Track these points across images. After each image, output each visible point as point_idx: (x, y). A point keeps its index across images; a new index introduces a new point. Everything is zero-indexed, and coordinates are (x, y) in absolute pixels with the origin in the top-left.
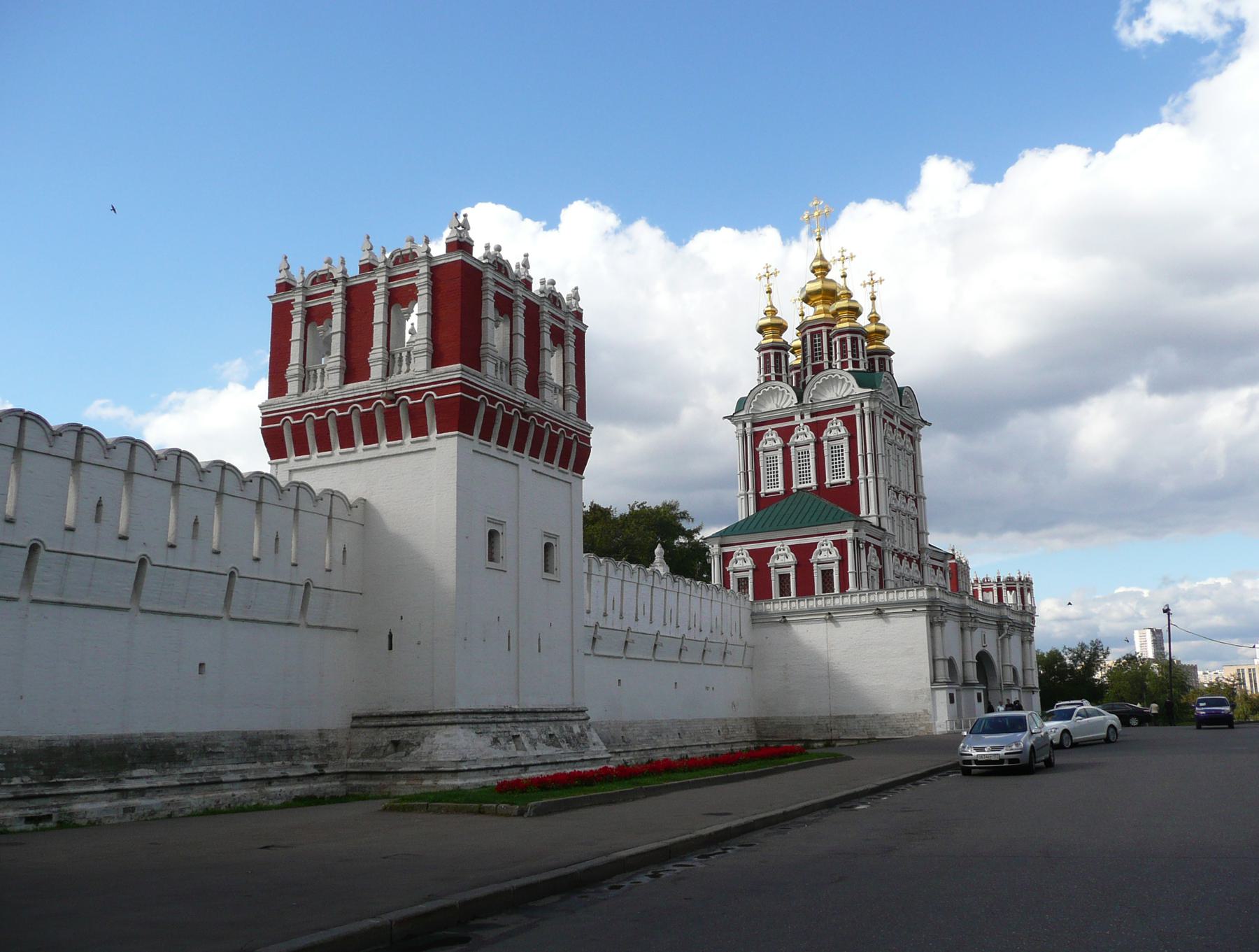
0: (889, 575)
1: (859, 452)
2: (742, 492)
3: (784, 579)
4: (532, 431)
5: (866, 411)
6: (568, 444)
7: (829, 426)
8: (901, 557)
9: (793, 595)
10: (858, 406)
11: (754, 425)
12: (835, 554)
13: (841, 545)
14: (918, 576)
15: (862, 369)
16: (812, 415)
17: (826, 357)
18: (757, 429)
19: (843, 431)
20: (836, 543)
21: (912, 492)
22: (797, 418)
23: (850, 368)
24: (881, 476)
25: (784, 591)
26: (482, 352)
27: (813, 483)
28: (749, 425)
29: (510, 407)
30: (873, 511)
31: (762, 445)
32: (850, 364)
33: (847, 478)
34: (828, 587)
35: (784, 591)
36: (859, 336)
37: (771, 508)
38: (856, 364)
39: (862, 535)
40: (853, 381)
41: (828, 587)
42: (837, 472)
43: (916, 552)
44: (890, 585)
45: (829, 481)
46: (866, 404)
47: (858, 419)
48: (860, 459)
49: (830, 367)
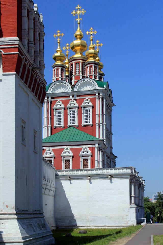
0: (106, 163)
1: (97, 113)
2: (46, 125)
3: (67, 161)
4: (34, 79)
5: (101, 97)
6: (41, 89)
7: (85, 101)
8: (107, 156)
9: (71, 168)
10: (97, 94)
11: (52, 98)
12: (90, 153)
13: (92, 150)
14: (110, 164)
15: (97, 79)
16: (77, 96)
17: (81, 73)
18: (52, 100)
19: (91, 104)
20: (90, 148)
21: (109, 130)
22: (71, 97)
23: (93, 78)
24: (104, 123)
25: (67, 166)
26: (23, 33)
27: (76, 124)
28: (50, 98)
29: (30, 66)
30: (101, 138)
31: (55, 107)
32: (93, 76)
33: (91, 123)
34: (85, 166)
35: (67, 166)
36: (97, 66)
37: (60, 132)
38: (95, 77)
39: (100, 146)
40: (96, 84)
41: (85, 166)
42: (87, 120)
43: (109, 154)
44: (106, 166)
45: (83, 123)
46: (101, 94)
47: (97, 100)
48: (97, 116)
49: (83, 77)
